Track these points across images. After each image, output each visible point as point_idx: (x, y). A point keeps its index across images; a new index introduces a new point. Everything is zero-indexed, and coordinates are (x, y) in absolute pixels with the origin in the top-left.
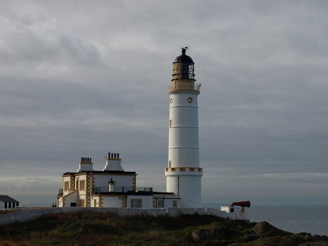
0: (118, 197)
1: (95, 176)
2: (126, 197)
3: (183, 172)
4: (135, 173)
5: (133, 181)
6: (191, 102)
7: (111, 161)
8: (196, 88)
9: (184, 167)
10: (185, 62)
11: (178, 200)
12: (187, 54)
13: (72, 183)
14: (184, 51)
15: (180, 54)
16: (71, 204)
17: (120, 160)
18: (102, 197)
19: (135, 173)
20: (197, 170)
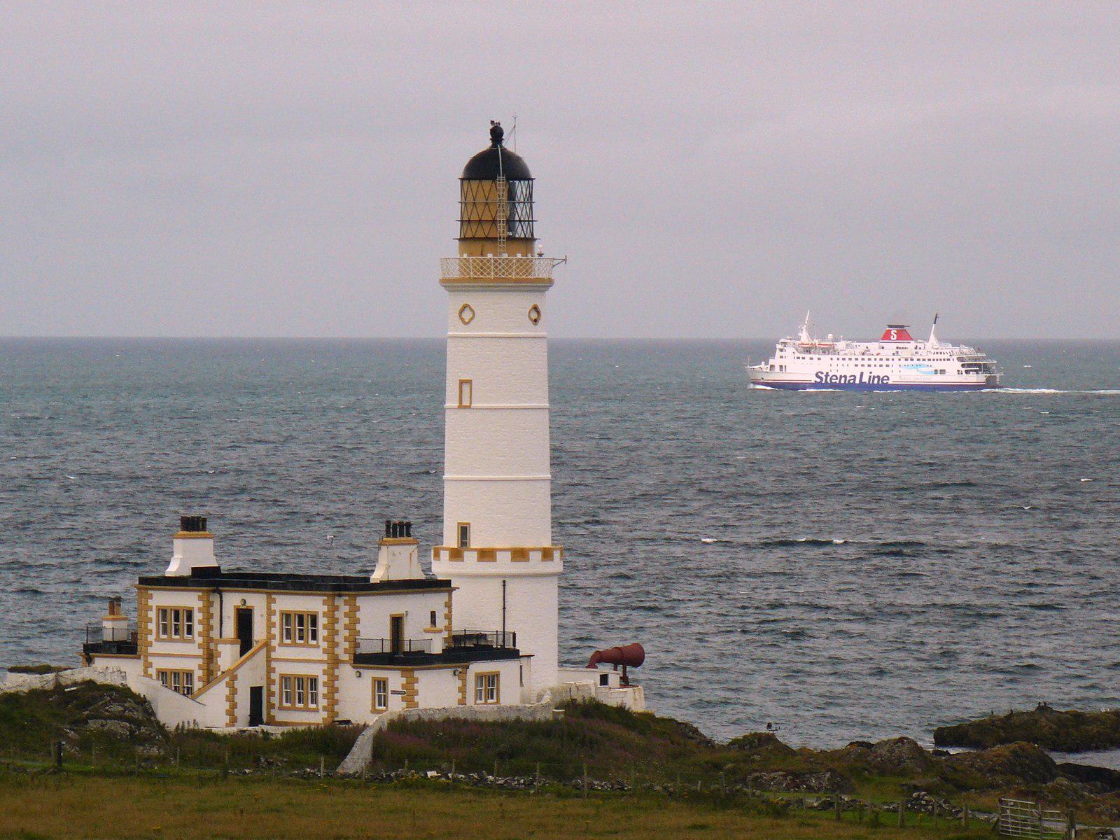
0: (450, 672)
4: (448, 583)
6: (535, 321)
12: (509, 144)
14: (497, 134)
15: (486, 144)
16: (251, 688)
18: (417, 674)
19: (448, 583)
20: (539, 555)
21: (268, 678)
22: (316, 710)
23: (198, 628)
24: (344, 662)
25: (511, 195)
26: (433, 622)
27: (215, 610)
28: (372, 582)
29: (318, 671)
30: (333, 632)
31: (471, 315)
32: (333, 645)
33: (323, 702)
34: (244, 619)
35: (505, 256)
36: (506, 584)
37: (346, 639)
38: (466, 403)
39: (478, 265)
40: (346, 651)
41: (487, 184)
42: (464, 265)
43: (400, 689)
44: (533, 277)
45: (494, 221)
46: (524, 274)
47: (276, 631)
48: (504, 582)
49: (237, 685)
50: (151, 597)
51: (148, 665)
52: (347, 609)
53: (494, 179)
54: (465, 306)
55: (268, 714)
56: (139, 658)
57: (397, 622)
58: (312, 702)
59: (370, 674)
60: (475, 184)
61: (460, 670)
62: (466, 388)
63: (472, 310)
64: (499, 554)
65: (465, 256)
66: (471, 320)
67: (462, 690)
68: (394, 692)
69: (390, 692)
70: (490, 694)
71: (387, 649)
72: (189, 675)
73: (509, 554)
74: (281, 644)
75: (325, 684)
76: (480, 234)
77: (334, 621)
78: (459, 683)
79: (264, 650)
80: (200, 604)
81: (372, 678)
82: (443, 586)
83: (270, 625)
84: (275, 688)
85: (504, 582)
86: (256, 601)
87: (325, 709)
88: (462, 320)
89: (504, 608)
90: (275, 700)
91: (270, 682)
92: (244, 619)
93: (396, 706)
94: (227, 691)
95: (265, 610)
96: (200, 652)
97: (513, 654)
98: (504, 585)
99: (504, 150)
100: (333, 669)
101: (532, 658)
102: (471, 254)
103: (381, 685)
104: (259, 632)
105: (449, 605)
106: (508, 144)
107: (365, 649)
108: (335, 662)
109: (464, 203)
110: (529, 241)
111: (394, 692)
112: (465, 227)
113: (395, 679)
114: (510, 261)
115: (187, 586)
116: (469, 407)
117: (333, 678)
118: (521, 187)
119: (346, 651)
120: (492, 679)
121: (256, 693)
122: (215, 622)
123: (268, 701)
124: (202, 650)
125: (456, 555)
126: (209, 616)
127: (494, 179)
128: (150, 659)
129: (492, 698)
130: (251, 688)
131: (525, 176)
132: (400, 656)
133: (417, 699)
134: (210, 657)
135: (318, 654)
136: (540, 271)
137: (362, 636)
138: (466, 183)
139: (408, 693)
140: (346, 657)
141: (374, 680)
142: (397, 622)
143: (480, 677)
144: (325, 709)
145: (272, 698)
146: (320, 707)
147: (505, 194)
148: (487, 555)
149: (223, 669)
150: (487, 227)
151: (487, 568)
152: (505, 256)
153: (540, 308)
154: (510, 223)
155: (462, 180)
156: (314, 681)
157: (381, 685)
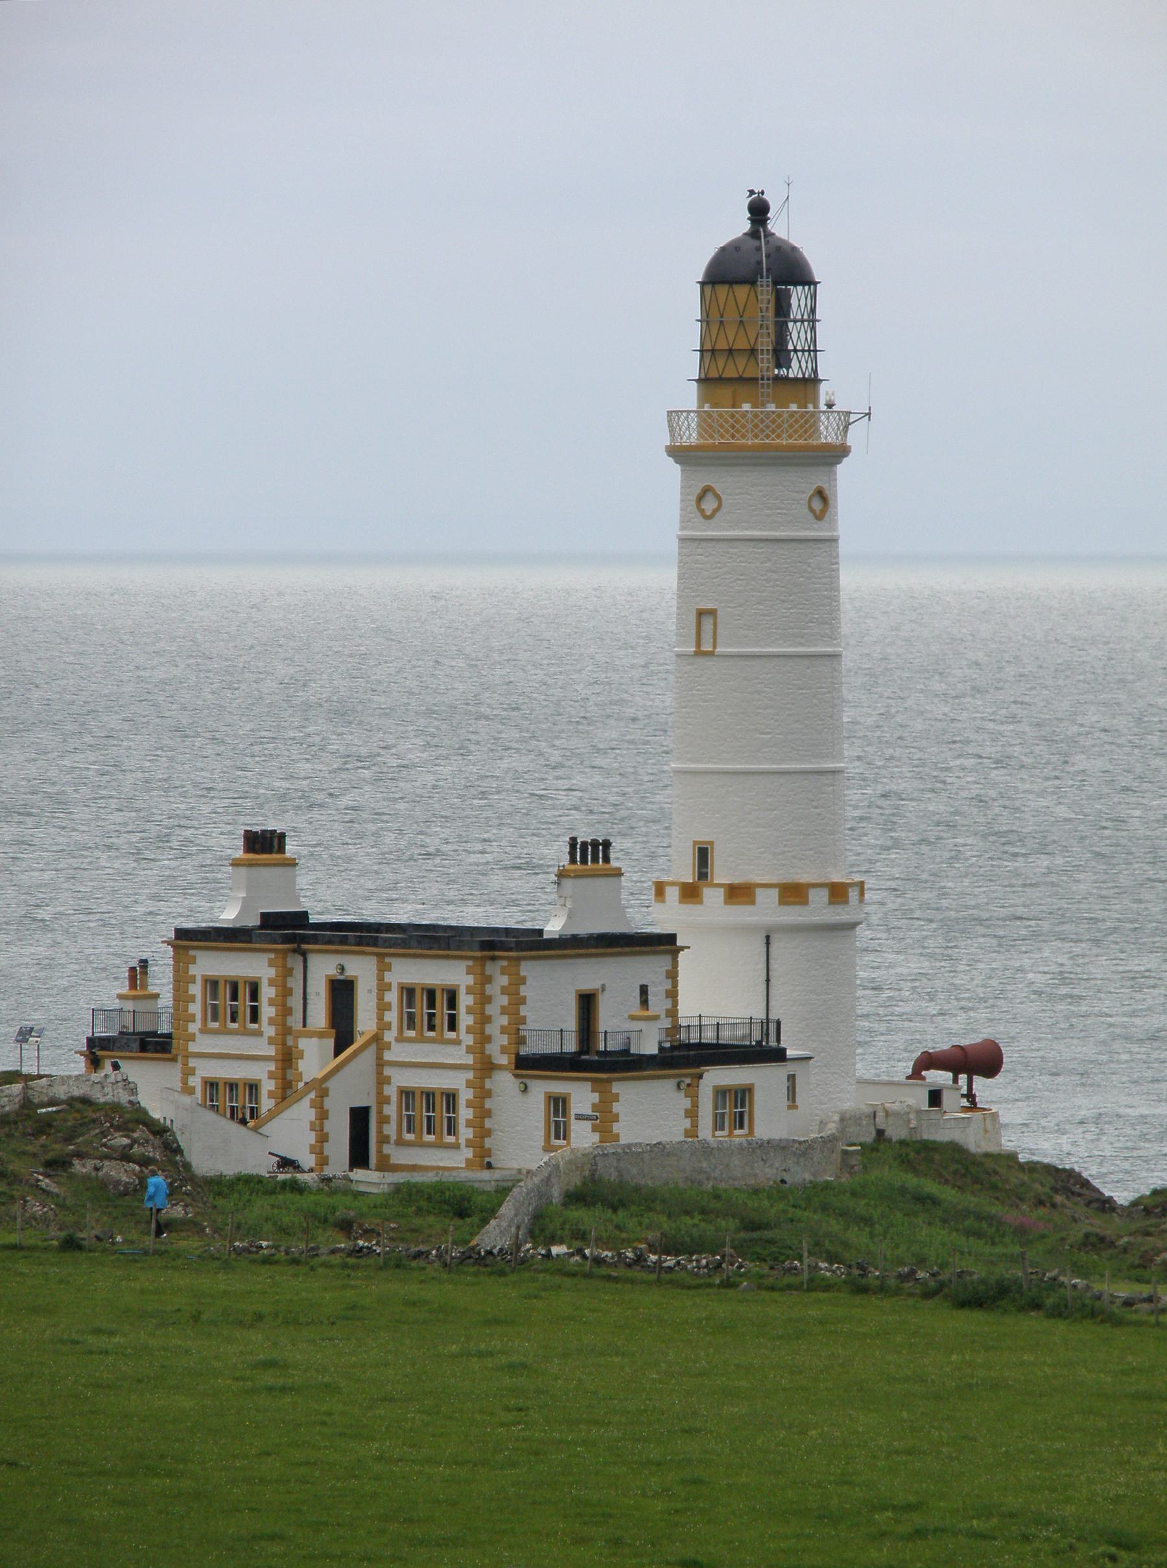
0: (670, 1084)
1: (527, 969)
3: (840, 909)
5: (668, 985)
8: (827, 433)
9: (804, 878)
14: (759, 211)
17: (618, 873)
18: (617, 1088)
19: (671, 939)
21: (380, 1092)
22: (456, 1146)
23: (267, 1011)
24: (500, 1067)
25: (782, 308)
26: (644, 1002)
27: (296, 983)
28: (545, 937)
29: (456, 1081)
31: (715, 505)
32: (484, 1039)
33: (465, 1133)
34: (342, 993)
35: (771, 407)
36: (772, 940)
37: (503, 1030)
38: (707, 647)
39: (726, 421)
40: (504, 1050)
41: (742, 291)
42: (706, 422)
43: (589, 1112)
44: (815, 443)
45: (753, 351)
46: (800, 437)
47: (392, 1017)
48: (768, 937)
49: (328, 1103)
50: (193, 960)
51: (188, 1072)
52: (504, 980)
53: (753, 283)
54: (706, 490)
55: (379, 1151)
56: (174, 1060)
57: (587, 1003)
58: (449, 1133)
59: (542, 1088)
60: (722, 290)
61: (688, 1081)
62: (707, 624)
63: (718, 497)
64: (760, 894)
65: (707, 407)
66: (715, 511)
67: (692, 1114)
68: (579, 1117)
69: (573, 1117)
70: (739, 1121)
71: (571, 1046)
72: (254, 1088)
73: (775, 893)
74: (400, 1039)
76: (731, 373)
77: (484, 1000)
78: (687, 1103)
79: (373, 1047)
80: (272, 972)
81: (546, 1093)
82: (665, 943)
83: (383, 1007)
84: (391, 1110)
85: (768, 937)
86: (361, 968)
87: (469, 1143)
88: (702, 511)
89: (768, 980)
90: (391, 1130)
92: (342, 993)
93: (583, 1137)
94: (311, 1115)
95: (374, 983)
96: (271, 1051)
97: (778, 1055)
98: (768, 943)
99: (769, 235)
100: (482, 1079)
101: (811, 1062)
102: (715, 405)
103: (558, 1104)
104: (365, 1021)
105: (673, 975)
106: (777, 226)
108: (486, 1067)
109: (706, 320)
110: (811, 382)
111: (579, 1117)
112: (707, 360)
113: (582, 1096)
114: (779, 415)
115: (250, 942)
116: (711, 654)
117: (483, 1093)
118: (798, 296)
119: (504, 1050)
120: (742, 1095)
121: (360, 1117)
122: (296, 1002)
123: (380, 1132)
124: (273, 1047)
125: (690, 893)
126: (286, 992)
127: (753, 283)
128: (192, 1063)
129: (741, 1127)
131: (806, 279)
132: (593, 1059)
133: (616, 1128)
134: (287, 1058)
136: (827, 433)
137: (530, 1024)
138: (708, 288)
139: (603, 1119)
140: (503, 1060)
142: (587, 1003)
143: (721, 1093)
144: (469, 1143)
145: (385, 1126)
146: (462, 1141)
147: (772, 306)
148: (739, 893)
149: (307, 1078)
150: (741, 362)
151: (742, 914)
152: (771, 407)
153: (827, 492)
154: (781, 355)
155: (703, 284)
156: (451, 1098)
157: (558, 1104)
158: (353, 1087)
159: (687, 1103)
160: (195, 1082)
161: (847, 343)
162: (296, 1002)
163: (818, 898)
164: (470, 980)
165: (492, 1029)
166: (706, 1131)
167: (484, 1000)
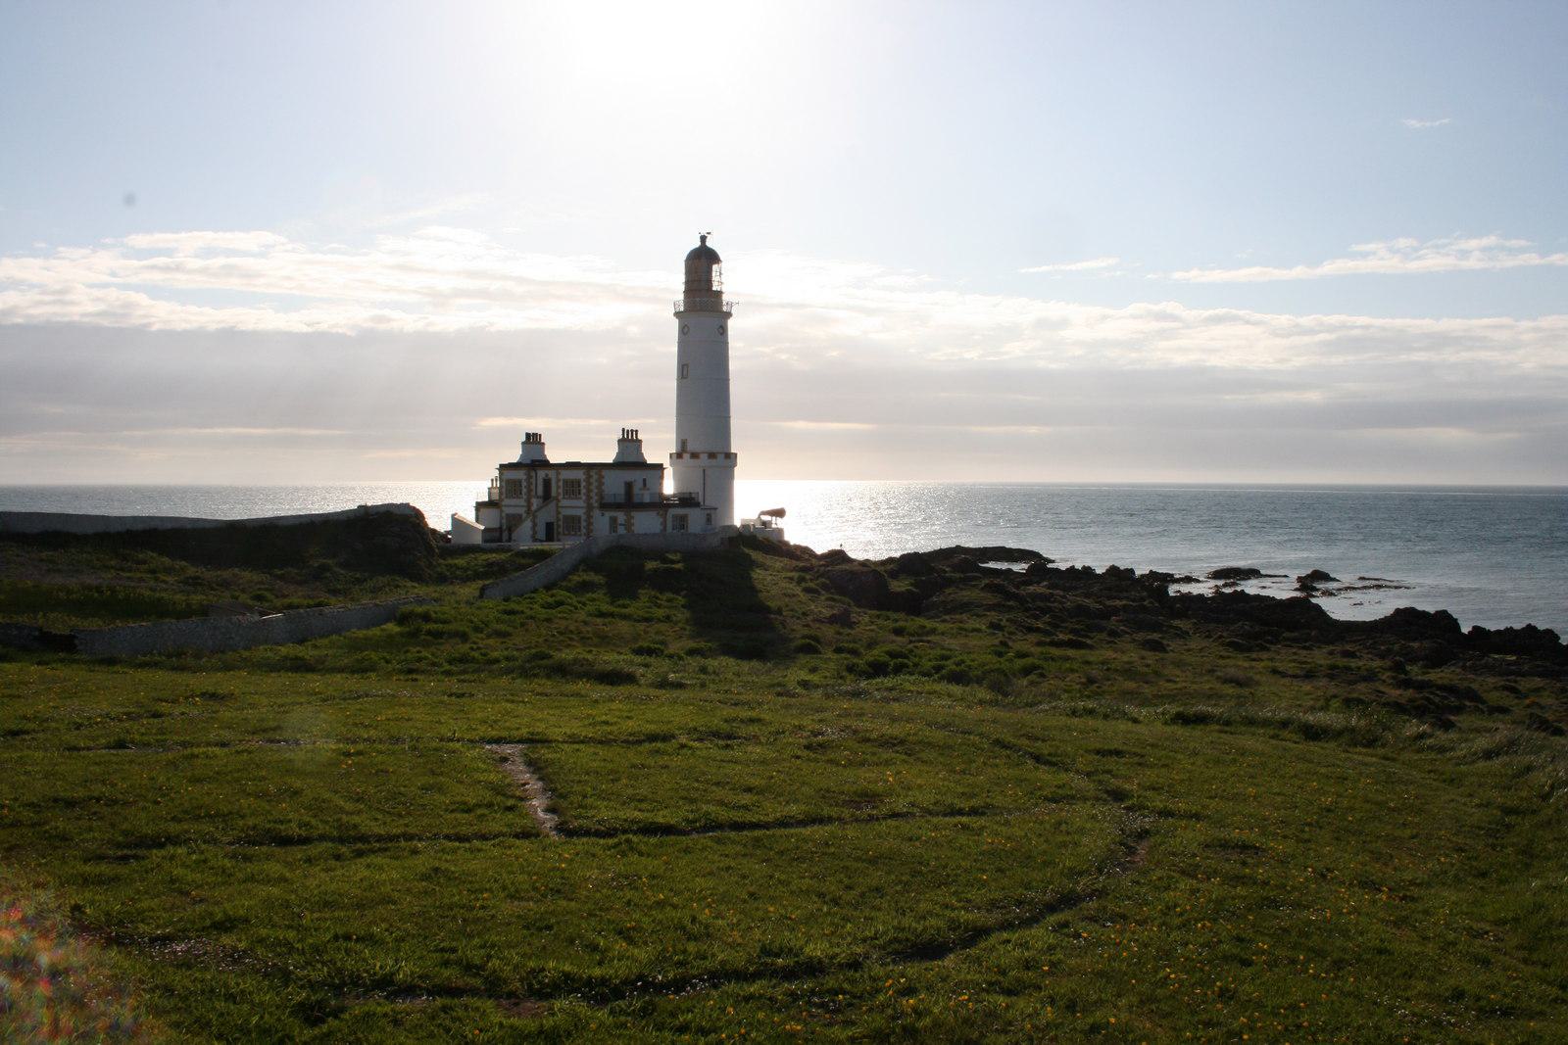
2: (667, 511)
4: (662, 465)
7: (626, 444)
10: (702, 261)
11: (713, 511)
12: (709, 244)
13: (529, 484)
14: (703, 239)
15: (697, 244)
18: (632, 514)
19: (662, 465)
20: (723, 455)
26: (645, 484)
29: (580, 512)
30: (589, 491)
33: (584, 531)
34: (547, 483)
37: (596, 495)
47: (561, 491)
49: (537, 521)
51: (502, 511)
57: (629, 486)
59: (608, 514)
64: (701, 456)
67: (664, 524)
68: (620, 525)
71: (621, 499)
74: (564, 498)
75: (585, 521)
77: (589, 484)
78: (661, 520)
80: (525, 477)
83: (558, 487)
84: (561, 523)
86: (552, 474)
90: (561, 530)
91: (558, 520)
92: (547, 483)
96: (525, 504)
97: (697, 505)
103: (613, 520)
107: (607, 500)
108: (590, 508)
111: (620, 525)
113: (621, 517)
117: (589, 517)
120: (683, 519)
122: (533, 487)
130: (547, 524)
135: (581, 503)
139: (628, 525)
140: (596, 505)
141: (611, 518)
143: (675, 517)
148: (694, 456)
157: (613, 520)
158: (546, 515)
159: (661, 520)
160: (504, 515)
161: (727, 280)
162: (533, 487)
163: (721, 457)
164: (584, 477)
165: (592, 494)
166: (669, 529)
167: (589, 484)
